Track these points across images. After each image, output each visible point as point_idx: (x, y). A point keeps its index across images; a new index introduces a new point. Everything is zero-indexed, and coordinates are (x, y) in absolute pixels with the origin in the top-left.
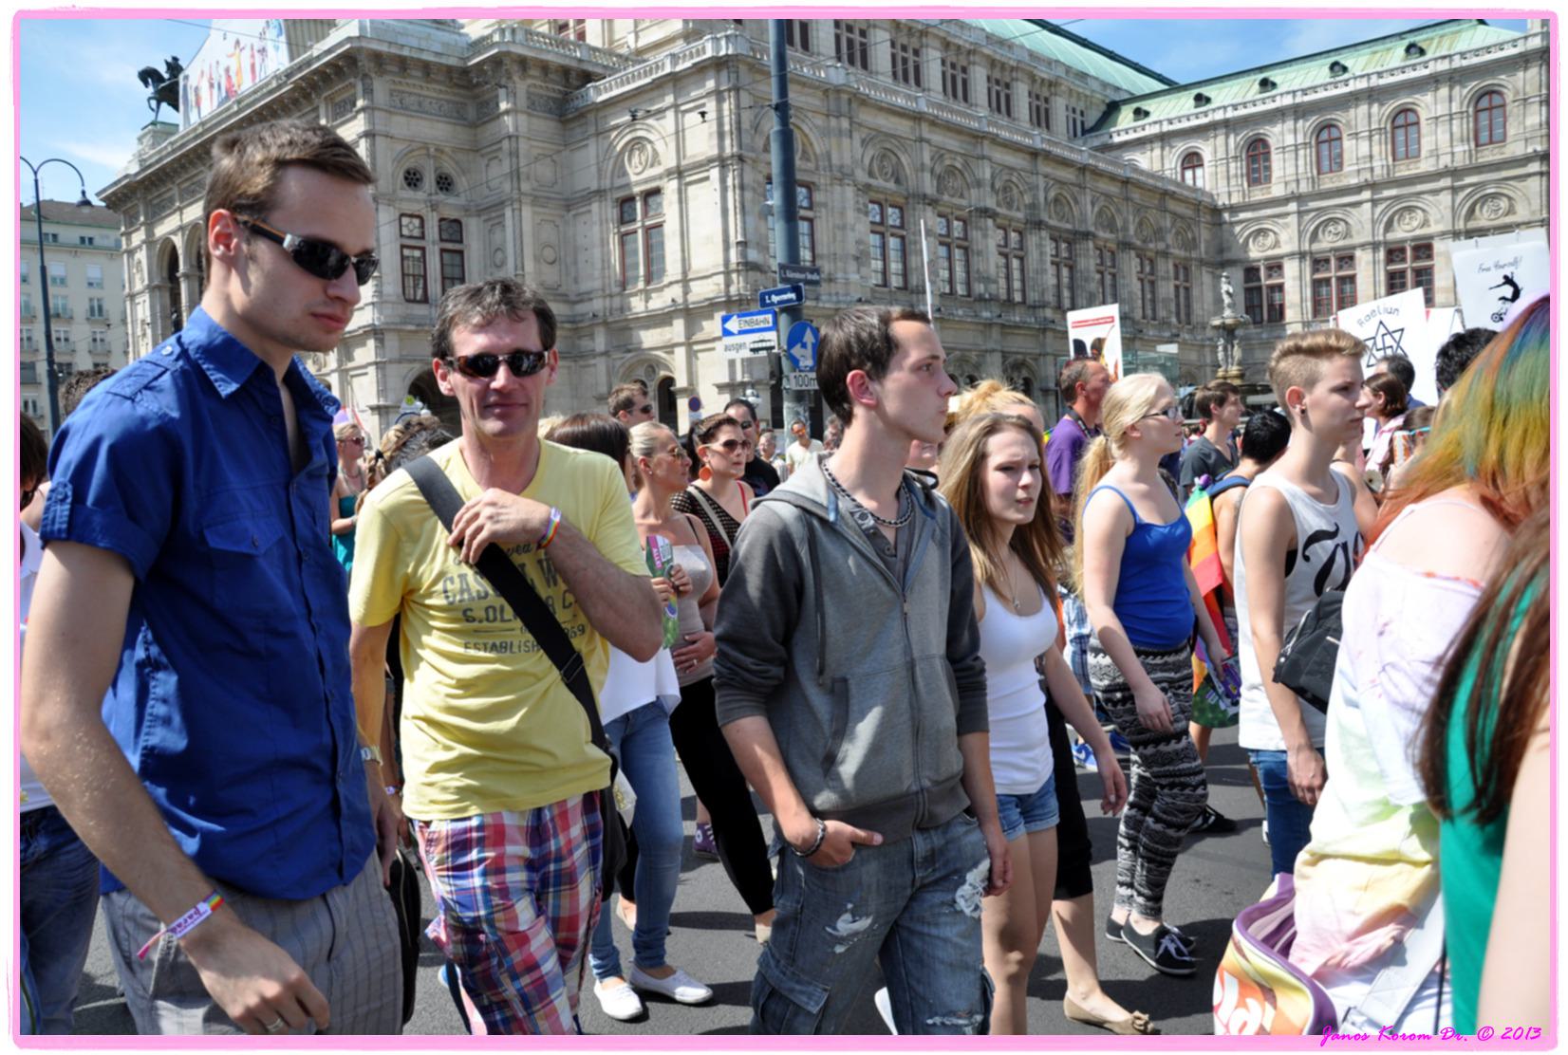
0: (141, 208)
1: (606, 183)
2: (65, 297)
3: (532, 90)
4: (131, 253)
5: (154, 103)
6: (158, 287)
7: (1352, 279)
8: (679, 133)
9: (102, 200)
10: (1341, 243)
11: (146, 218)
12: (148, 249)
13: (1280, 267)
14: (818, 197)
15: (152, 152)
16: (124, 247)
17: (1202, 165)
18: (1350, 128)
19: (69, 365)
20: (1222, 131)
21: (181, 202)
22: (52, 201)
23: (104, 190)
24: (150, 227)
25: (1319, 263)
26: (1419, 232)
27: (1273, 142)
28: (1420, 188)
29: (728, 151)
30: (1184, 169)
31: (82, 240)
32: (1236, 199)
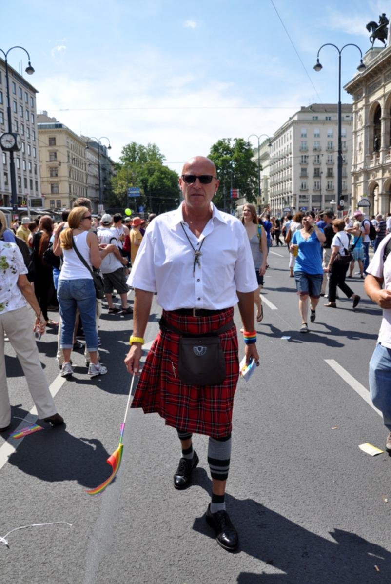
0: (364, 90)
2: (319, 142)
4: (357, 112)
5: (372, 39)
6: (369, 126)
9: (346, 90)
11: (366, 95)
12: (366, 108)
15: (370, 62)
16: (354, 110)
19: (319, 169)
21: (385, 82)
22: (316, 104)
23: (347, 84)
24: (367, 98)
31: (326, 118)
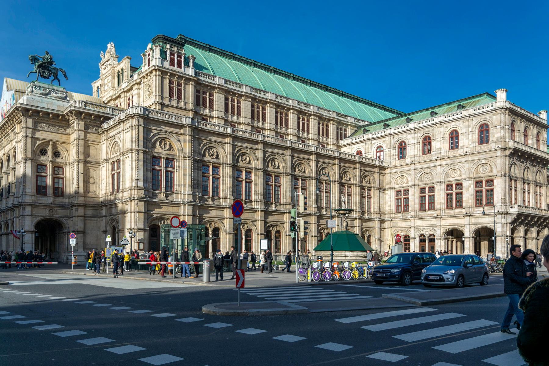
1: (109, 157)
3: (87, 123)
7: (434, 195)
8: (124, 141)
10: (429, 182)
13: (408, 190)
14: (176, 164)
17: (383, 151)
18: (434, 137)
20: (389, 137)
25: (423, 190)
26: (457, 178)
27: (407, 142)
28: (458, 160)
29: (134, 147)
30: (377, 152)
32: (393, 164)
